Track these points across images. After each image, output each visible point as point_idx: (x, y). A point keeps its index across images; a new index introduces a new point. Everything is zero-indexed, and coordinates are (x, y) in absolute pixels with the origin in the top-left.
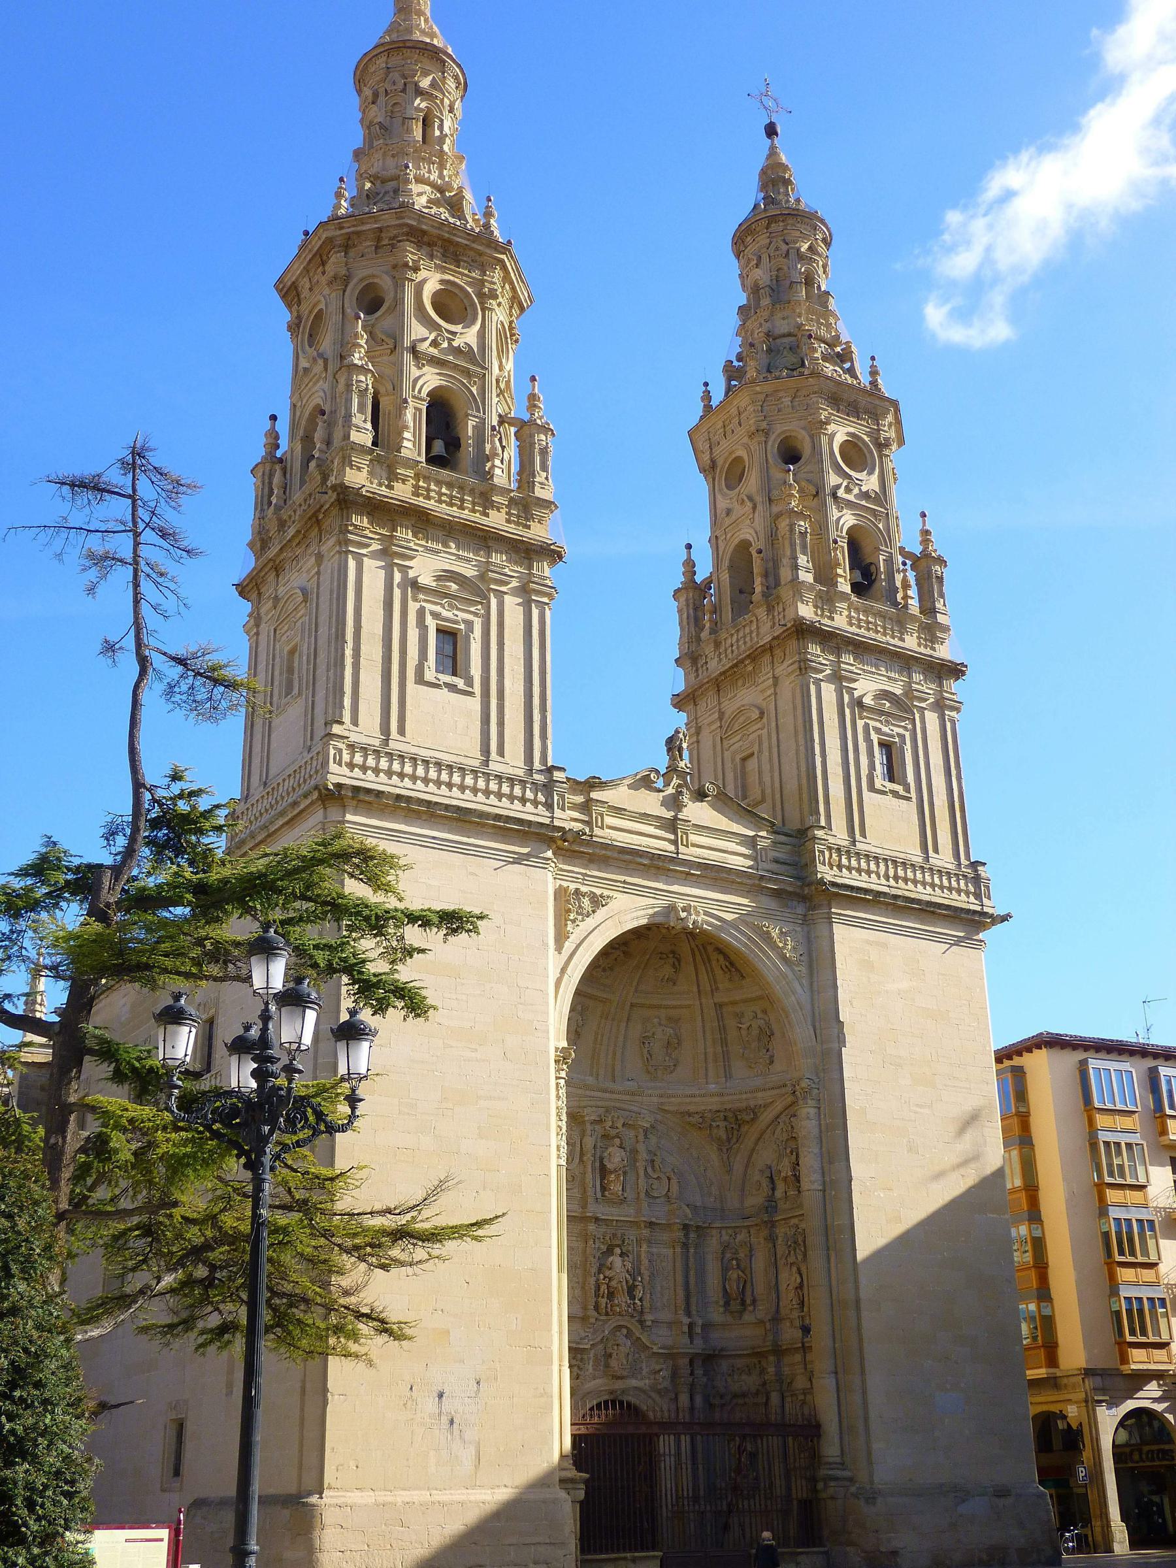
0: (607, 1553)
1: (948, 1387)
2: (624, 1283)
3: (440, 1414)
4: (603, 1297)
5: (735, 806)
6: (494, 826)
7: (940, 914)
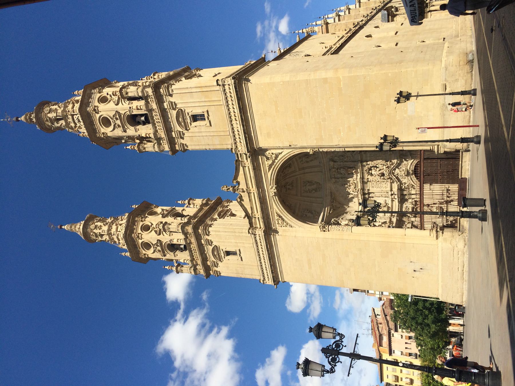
0: (459, 166)
1: (405, 109)
2: (380, 172)
3: (420, 271)
4: (384, 178)
5: (236, 173)
6: (270, 250)
7: (242, 106)
